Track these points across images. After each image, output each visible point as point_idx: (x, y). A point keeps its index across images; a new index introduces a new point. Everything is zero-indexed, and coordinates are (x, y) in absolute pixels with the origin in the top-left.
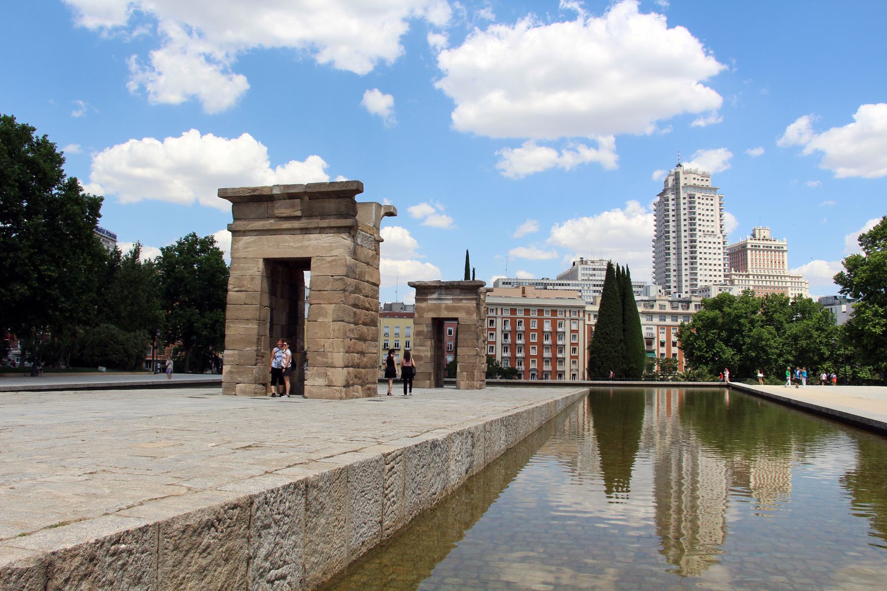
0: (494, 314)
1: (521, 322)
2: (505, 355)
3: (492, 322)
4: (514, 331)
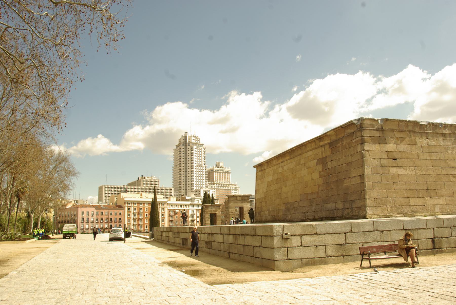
0: (130, 205)
1: (141, 209)
2: (134, 223)
3: (129, 209)
4: (139, 213)
